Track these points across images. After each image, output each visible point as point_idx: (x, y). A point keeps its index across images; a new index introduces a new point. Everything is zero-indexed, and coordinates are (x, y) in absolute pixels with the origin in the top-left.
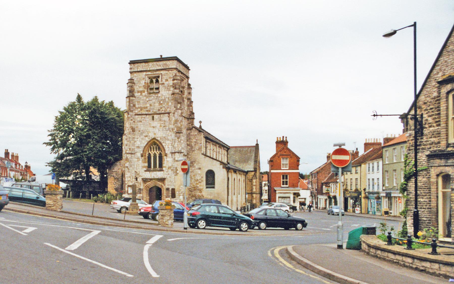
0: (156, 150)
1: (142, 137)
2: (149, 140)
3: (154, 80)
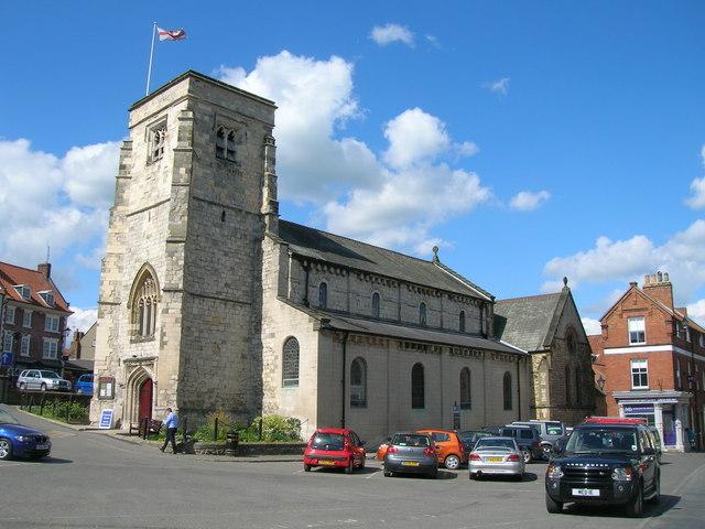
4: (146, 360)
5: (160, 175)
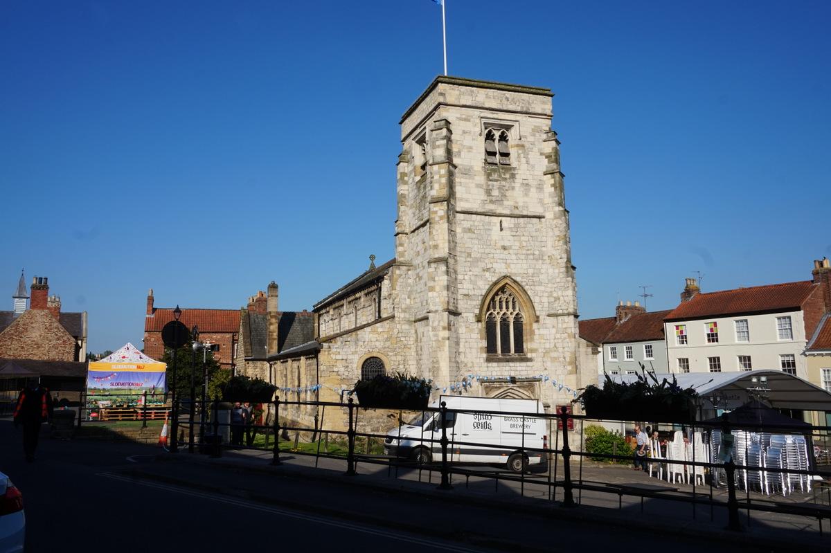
0: (507, 308)
1: (477, 271)
2: (494, 279)
3: (497, 134)
4: (522, 381)
5: (517, 184)
